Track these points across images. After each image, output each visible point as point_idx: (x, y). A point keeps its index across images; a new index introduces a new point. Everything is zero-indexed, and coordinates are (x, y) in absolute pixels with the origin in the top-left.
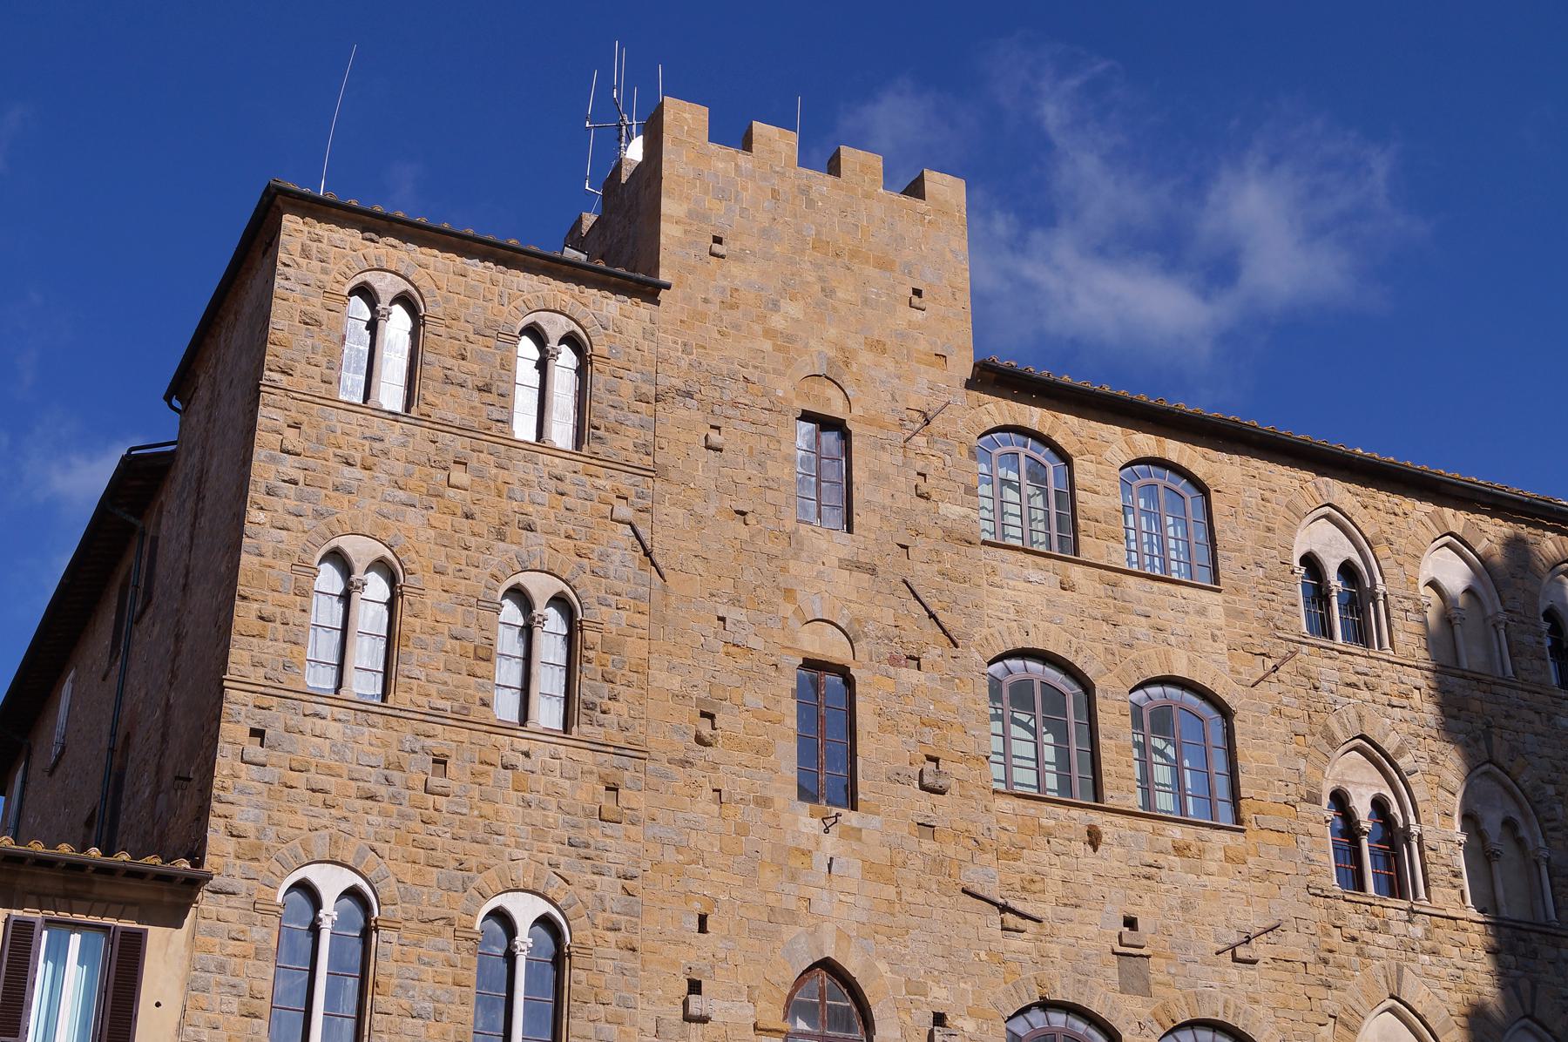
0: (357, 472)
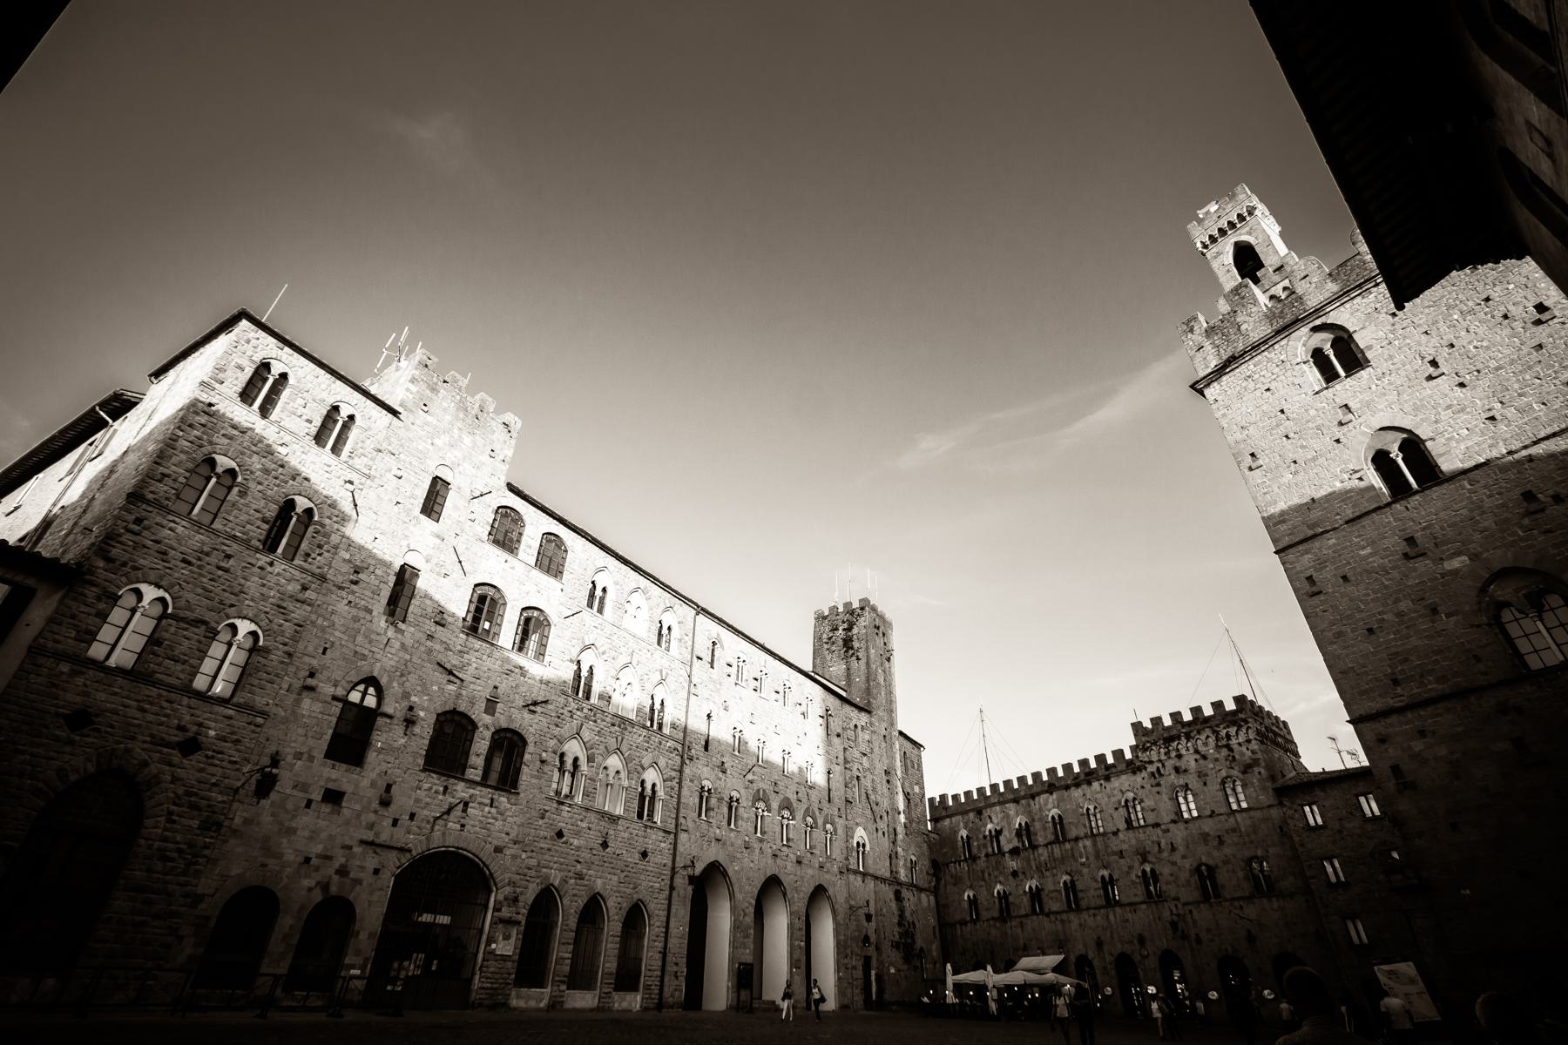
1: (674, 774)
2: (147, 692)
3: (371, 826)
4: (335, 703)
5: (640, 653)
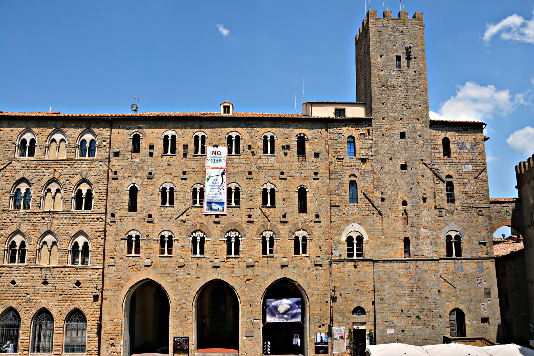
1: (99, 234)
5: (62, 168)
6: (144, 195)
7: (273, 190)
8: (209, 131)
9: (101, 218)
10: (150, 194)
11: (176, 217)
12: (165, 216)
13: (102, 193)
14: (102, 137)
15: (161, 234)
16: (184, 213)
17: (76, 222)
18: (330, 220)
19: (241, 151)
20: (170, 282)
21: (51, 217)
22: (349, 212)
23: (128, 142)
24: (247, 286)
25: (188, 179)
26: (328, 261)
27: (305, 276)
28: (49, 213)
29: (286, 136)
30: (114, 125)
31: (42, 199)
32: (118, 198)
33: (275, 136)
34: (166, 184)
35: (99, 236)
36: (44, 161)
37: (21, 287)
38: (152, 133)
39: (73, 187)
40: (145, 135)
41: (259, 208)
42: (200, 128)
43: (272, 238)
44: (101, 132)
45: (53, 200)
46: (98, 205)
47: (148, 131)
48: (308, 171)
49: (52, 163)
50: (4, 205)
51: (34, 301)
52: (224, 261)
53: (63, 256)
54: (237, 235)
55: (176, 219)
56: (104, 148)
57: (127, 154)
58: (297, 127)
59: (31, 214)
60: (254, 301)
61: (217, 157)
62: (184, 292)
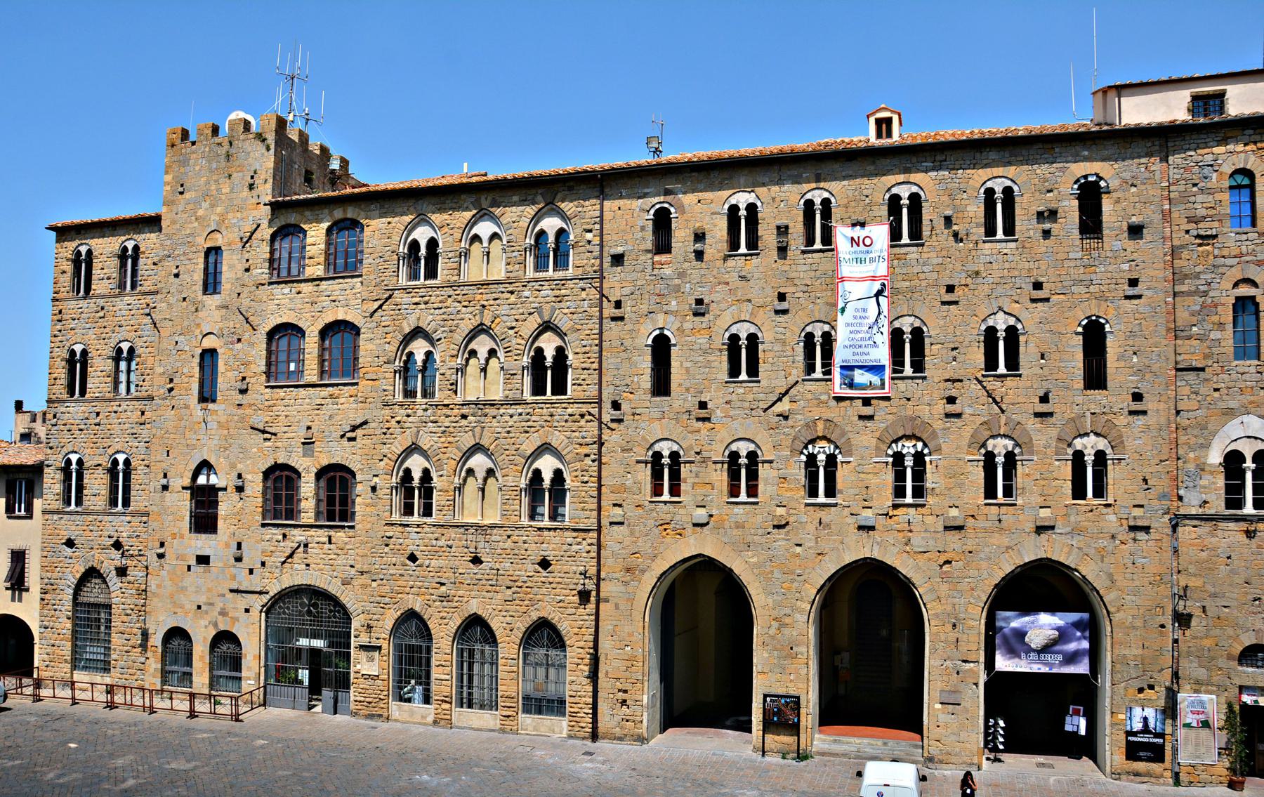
0: (76, 321)
1: (586, 450)
2: (90, 519)
3: (234, 577)
4: (185, 491)
5: (498, 302)
6: (688, 355)
7: (1012, 333)
8: (841, 186)
9: (590, 414)
10: (701, 353)
11: (766, 406)
12: (739, 404)
13: (589, 355)
14: (583, 221)
15: (729, 448)
16: (784, 395)
17: (534, 424)
18: (1173, 407)
19: (924, 233)
20: (755, 564)
21: (480, 414)
22: (1231, 384)
23: (643, 228)
24: (944, 577)
25: (792, 312)
26: (1168, 517)
27: (1102, 555)
28: (476, 404)
29: (1046, 184)
30: (607, 190)
31: (460, 373)
32: (626, 365)
33: (1016, 188)
34: (738, 325)
35: (587, 455)
36: (459, 286)
37: (429, 569)
38: (699, 202)
39: (524, 342)
40: (680, 208)
41: (977, 379)
42: (818, 180)
43: (1010, 457)
44: (580, 209)
45: (483, 374)
46: (582, 382)
47: (688, 199)
48: (1109, 275)
49: (476, 291)
50: (385, 390)
51: (456, 599)
52: (887, 515)
53: (511, 501)
54: (919, 449)
55: (765, 410)
56: (589, 247)
57: (642, 258)
58: (1078, 158)
59: (439, 407)
60: (962, 616)
61: (862, 252)
62: (788, 589)
